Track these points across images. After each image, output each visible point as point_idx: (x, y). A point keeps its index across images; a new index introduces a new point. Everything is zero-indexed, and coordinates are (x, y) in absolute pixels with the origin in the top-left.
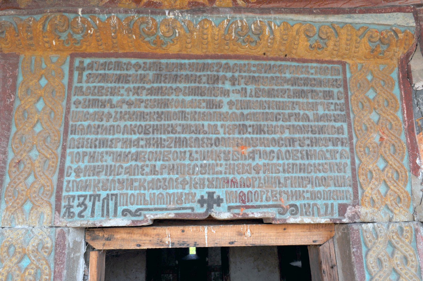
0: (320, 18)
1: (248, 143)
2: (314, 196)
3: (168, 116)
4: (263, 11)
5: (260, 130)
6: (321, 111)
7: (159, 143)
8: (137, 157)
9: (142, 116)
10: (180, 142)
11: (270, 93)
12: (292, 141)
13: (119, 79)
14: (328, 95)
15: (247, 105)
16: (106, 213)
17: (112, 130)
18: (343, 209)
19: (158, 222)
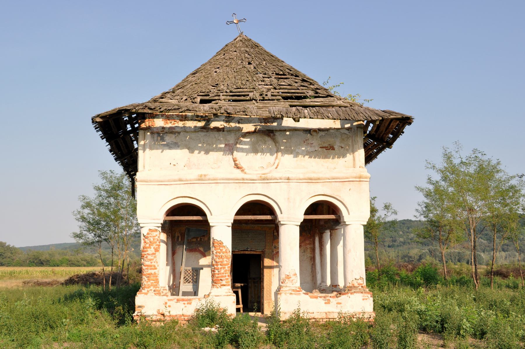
0: (262, 225)
1: (252, 241)
2: (260, 248)
3: (242, 238)
4: (255, 224)
5: (254, 239)
6: (262, 237)
7: (241, 241)
8: (239, 243)
9: (239, 237)
10: (244, 241)
11: (255, 235)
12: (258, 241)
13: (237, 232)
14: (263, 235)
15: (252, 236)
16: (235, 249)
17: (236, 239)
18: (263, 250)
19: (241, 251)
